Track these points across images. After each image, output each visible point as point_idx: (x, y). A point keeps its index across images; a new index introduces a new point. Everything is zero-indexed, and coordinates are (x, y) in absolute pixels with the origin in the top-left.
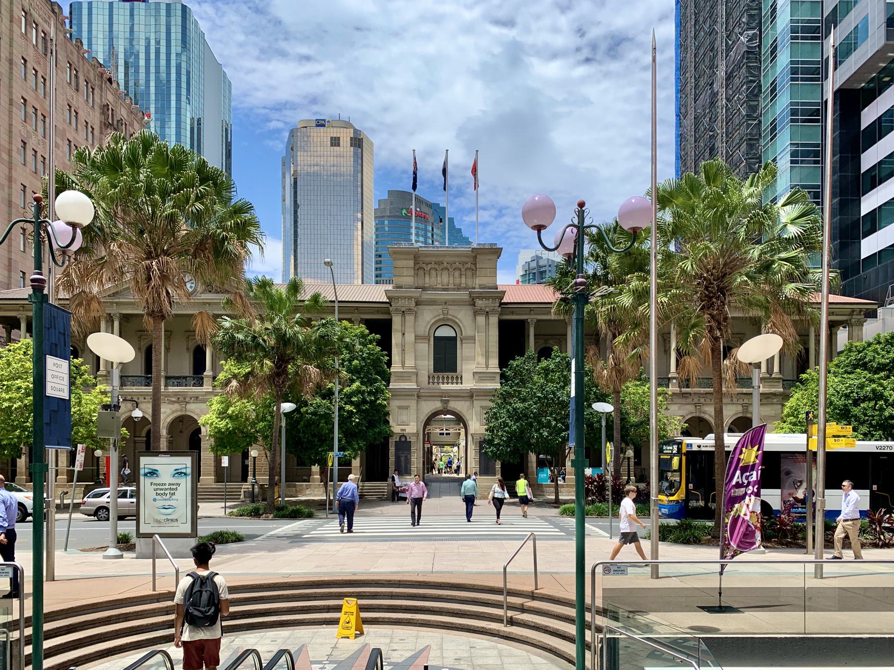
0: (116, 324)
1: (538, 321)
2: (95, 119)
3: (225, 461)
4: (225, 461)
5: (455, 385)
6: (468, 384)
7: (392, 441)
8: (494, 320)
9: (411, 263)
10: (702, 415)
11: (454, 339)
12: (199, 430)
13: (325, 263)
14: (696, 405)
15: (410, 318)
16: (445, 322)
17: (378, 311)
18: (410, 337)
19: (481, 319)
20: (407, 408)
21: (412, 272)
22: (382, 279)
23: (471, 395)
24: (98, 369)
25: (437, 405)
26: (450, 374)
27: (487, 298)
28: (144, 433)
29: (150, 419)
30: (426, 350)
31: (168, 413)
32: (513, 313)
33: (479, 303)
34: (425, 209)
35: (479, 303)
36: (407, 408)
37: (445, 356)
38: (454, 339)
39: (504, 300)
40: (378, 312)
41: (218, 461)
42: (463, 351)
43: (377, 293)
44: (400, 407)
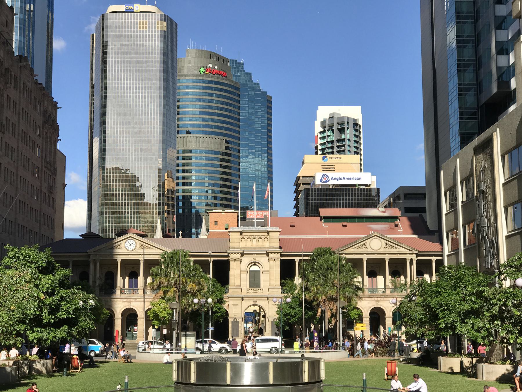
2: (40, 121)
6: (266, 293)
7: (230, 321)
8: (278, 263)
11: (259, 271)
16: (255, 263)
18: (238, 271)
19: (272, 262)
20: (237, 305)
26: (257, 289)
27: (275, 253)
30: (246, 277)
33: (270, 255)
35: (270, 255)
36: (237, 305)
37: (255, 280)
38: (259, 271)
42: (263, 277)
44: (234, 305)
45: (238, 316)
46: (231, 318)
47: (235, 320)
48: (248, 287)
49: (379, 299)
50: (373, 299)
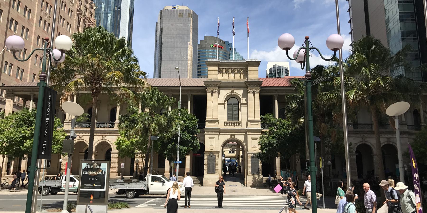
0: (75, 98)
1: (279, 95)
3: (123, 164)
4: (123, 164)
5: (238, 127)
6: (244, 127)
7: (206, 156)
9: (216, 68)
10: (366, 143)
12: (111, 149)
13: (176, 69)
14: (363, 138)
15: (215, 95)
17: (200, 91)
18: (216, 104)
19: (250, 95)
21: (217, 72)
22: (201, 76)
23: (246, 132)
24: (65, 119)
25: (228, 137)
28: (84, 151)
29: (88, 145)
31: (97, 139)
32: (266, 92)
34: (223, 45)
36: (213, 138)
39: (262, 86)
40: (200, 91)
41: (119, 165)
43: (200, 83)
44: (210, 138)
45: (215, 150)
46: (208, 152)
47: (212, 155)
48: (226, 120)
49: (365, 135)
50: (359, 135)
